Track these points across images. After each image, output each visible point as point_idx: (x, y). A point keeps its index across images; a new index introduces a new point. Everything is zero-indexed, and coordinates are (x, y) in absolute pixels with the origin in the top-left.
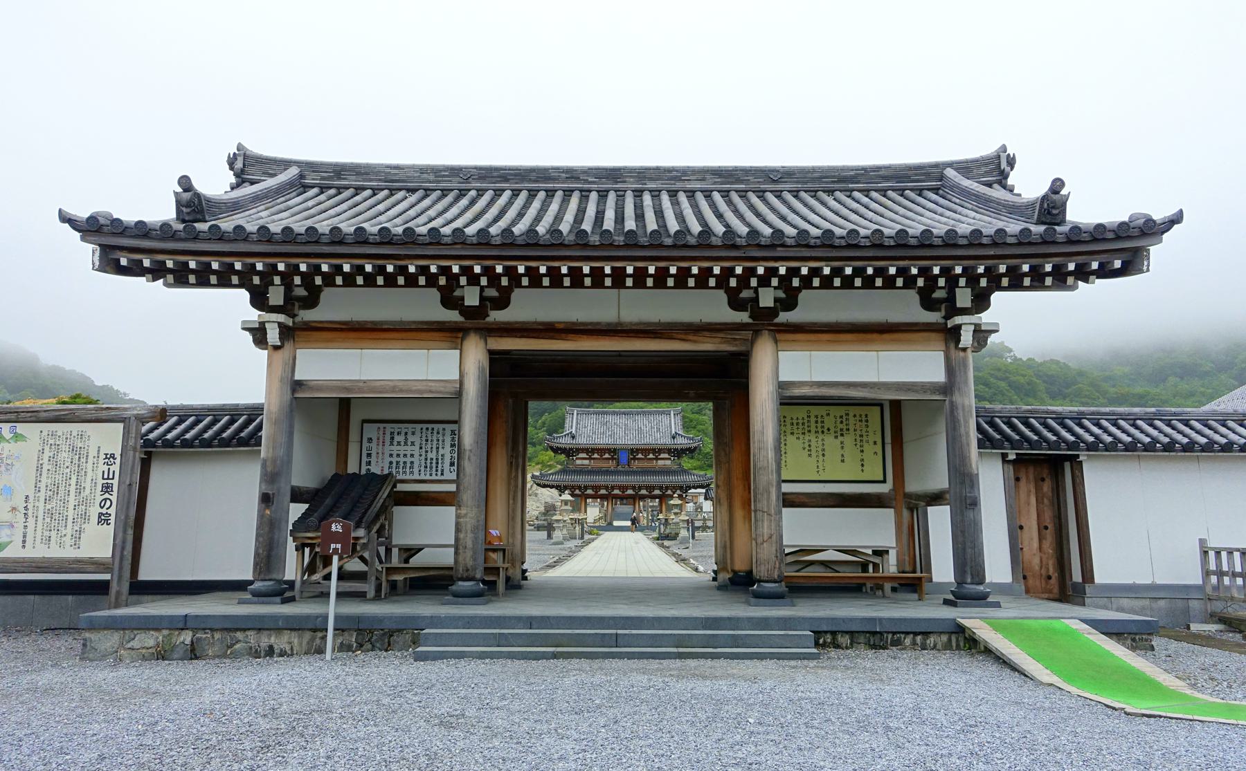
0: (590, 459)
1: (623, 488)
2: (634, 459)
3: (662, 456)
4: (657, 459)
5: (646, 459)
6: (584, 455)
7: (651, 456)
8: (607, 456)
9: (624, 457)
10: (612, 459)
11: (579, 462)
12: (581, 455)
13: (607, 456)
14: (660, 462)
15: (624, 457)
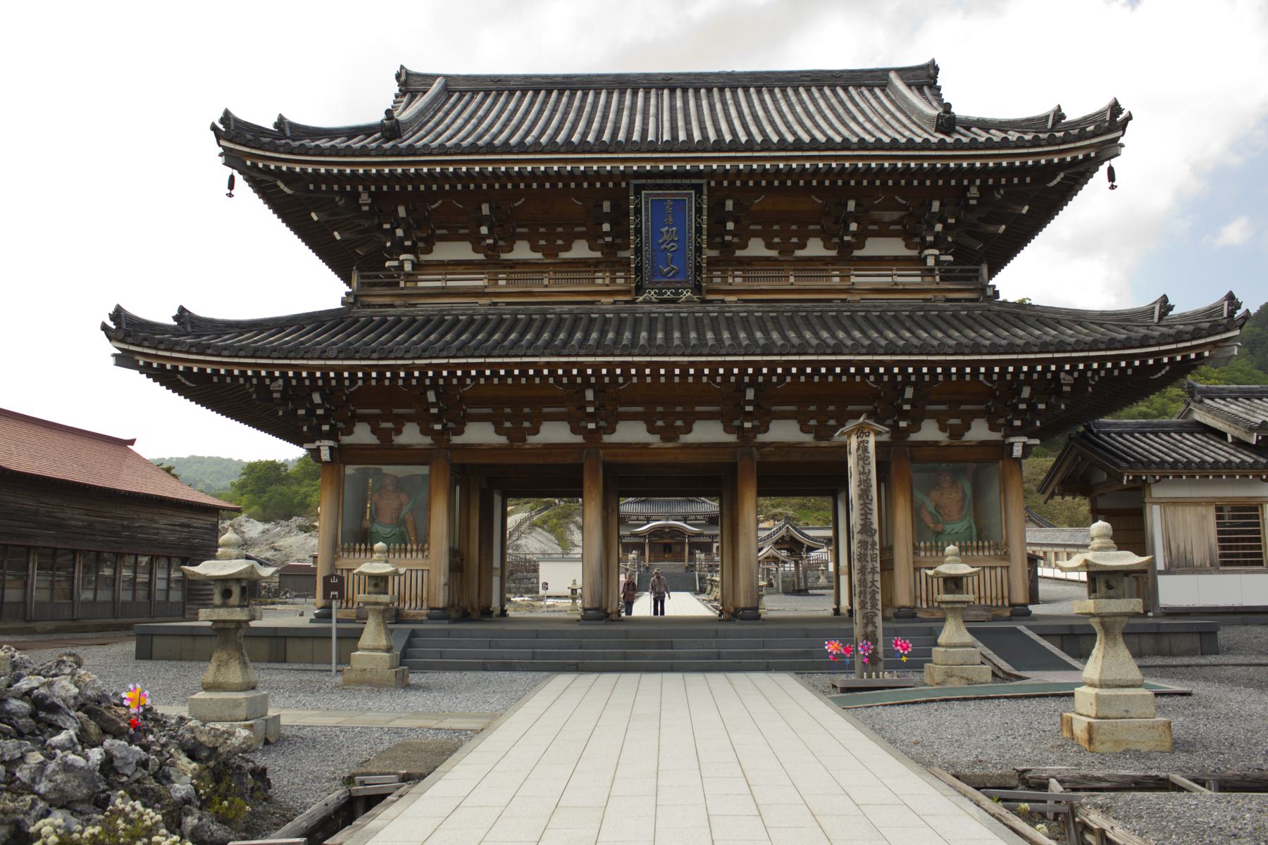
0: (492, 263)
1: (668, 401)
2: (728, 261)
3: (875, 247)
4: (846, 258)
5: (786, 261)
6: (462, 251)
7: (815, 248)
8: (580, 250)
9: (670, 229)
10: (611, 262)
11: (428, 282)
12: (445, 251)
13: (580, 250)
14: (861, 280)
15: (670, 229)
